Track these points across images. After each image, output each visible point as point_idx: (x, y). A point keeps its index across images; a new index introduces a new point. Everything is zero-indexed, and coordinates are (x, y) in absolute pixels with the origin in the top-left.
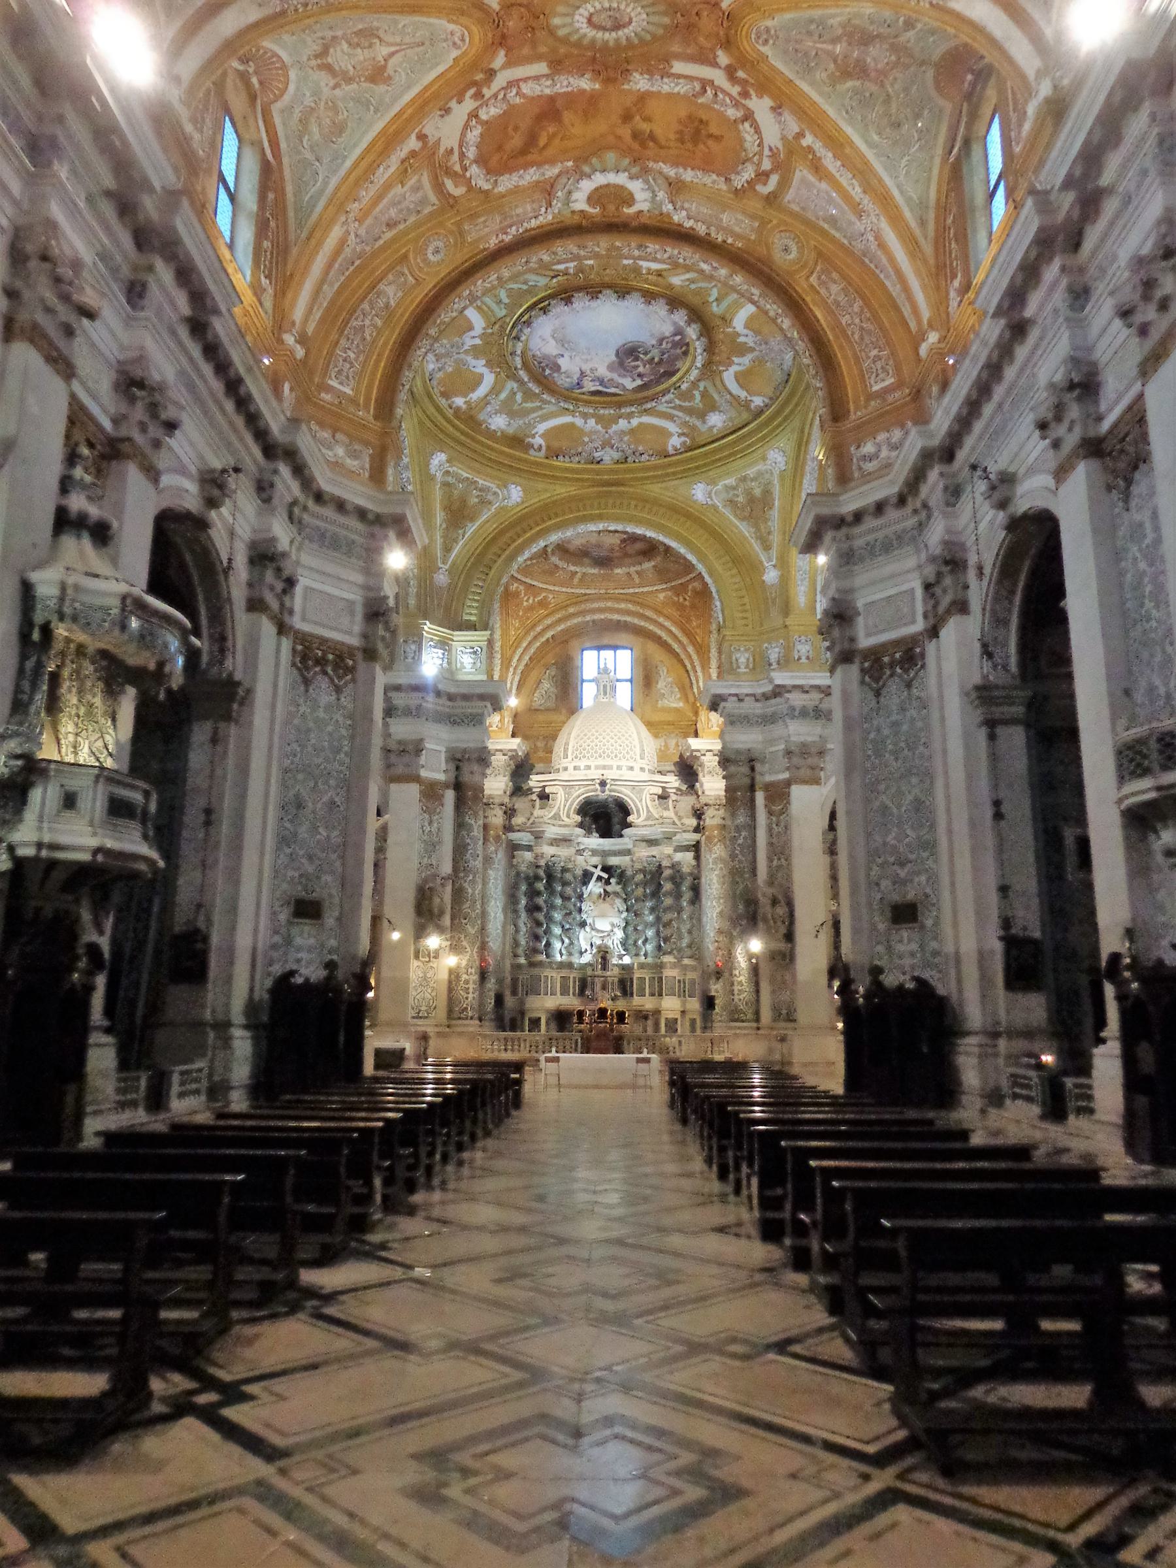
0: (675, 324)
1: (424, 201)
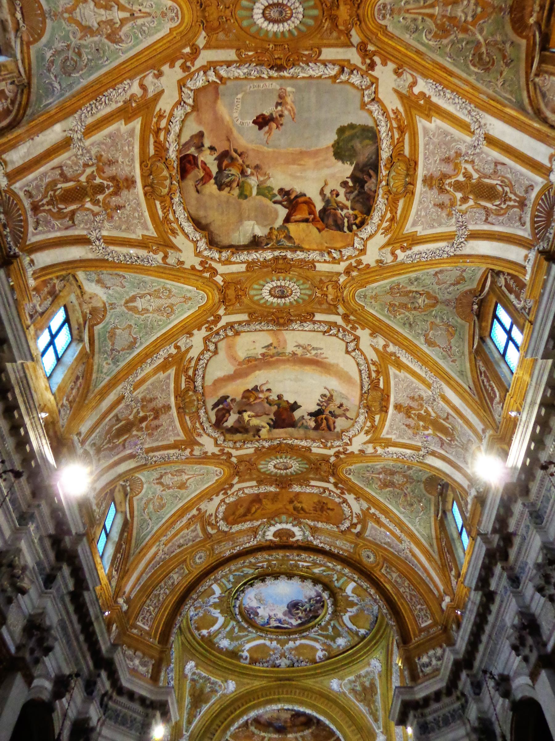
0: (316, 591)
1: (197, 536)
